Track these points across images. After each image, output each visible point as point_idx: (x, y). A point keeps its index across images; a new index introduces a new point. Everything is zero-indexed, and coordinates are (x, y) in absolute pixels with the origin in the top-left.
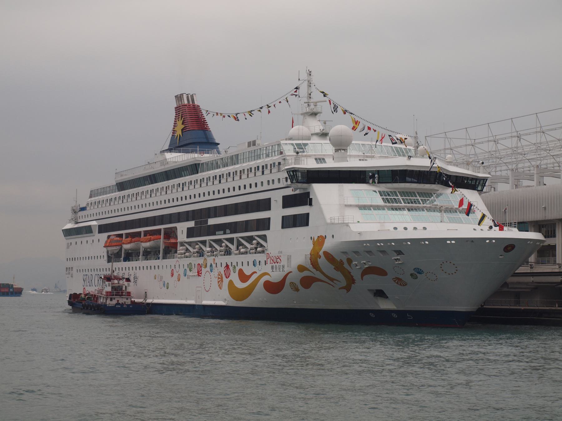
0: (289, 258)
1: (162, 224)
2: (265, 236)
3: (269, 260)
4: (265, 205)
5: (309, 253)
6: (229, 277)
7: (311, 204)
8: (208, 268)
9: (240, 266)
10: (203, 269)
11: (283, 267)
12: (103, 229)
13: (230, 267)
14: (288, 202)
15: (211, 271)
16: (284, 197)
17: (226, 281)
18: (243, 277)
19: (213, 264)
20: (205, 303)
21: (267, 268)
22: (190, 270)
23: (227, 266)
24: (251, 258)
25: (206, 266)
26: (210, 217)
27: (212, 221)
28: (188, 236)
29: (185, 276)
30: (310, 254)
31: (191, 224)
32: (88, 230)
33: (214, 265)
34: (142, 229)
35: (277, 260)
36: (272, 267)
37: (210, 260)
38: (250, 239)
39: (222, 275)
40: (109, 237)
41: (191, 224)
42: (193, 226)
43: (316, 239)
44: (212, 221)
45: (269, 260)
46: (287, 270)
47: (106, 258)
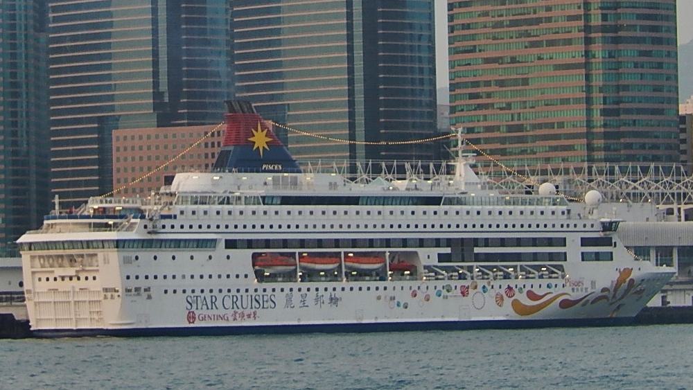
0: (593, 283)
1: (388, 246)
2: (562, 266)
3: (568, 284)
4: (563, 242)
5: (616, 280)
6: (512, 296)
7: (615, 246)
8: (480, 288)
9: (528, 288)
10: (470, 290)
11: (586, 289)
12: (231, 244)
13: (514, 288)
14: (585, 242)
15: (485, 292)
16: (582, 238)
17: (508, 302)
18: (531, 295)
19: (487, 286)
20: (473, 319)
21: (568, 289)
22: (448, 291)
23: (510, 288)
24: (545, 282)
25: (476, 287)
26: (477, 246)
27: (477, 250)
28: (439, 261)
29: (440, 296)
30: (618, 281)
31: (448, 250)
32: (212, 243)
33: (489, 288)
34: (342, 250)
35: (578, 283)
36: (573, 289)
37: (481, 283)
38: (538, 268)
39: (502, 295)
40: (255, 256)
41: (448, 250)
42: (450, 252)
43: (622, 270)
44: (477, 250)
45: (568, 284)
46: (590, 291)
47: (252, 275)
